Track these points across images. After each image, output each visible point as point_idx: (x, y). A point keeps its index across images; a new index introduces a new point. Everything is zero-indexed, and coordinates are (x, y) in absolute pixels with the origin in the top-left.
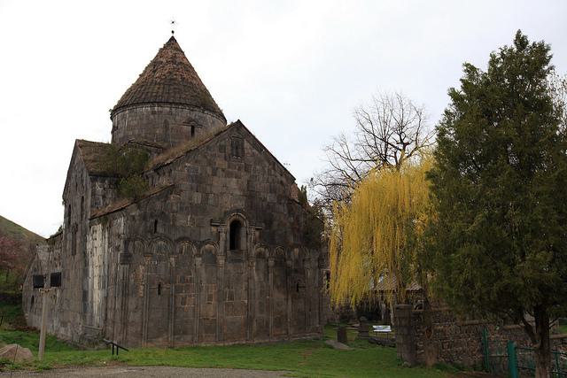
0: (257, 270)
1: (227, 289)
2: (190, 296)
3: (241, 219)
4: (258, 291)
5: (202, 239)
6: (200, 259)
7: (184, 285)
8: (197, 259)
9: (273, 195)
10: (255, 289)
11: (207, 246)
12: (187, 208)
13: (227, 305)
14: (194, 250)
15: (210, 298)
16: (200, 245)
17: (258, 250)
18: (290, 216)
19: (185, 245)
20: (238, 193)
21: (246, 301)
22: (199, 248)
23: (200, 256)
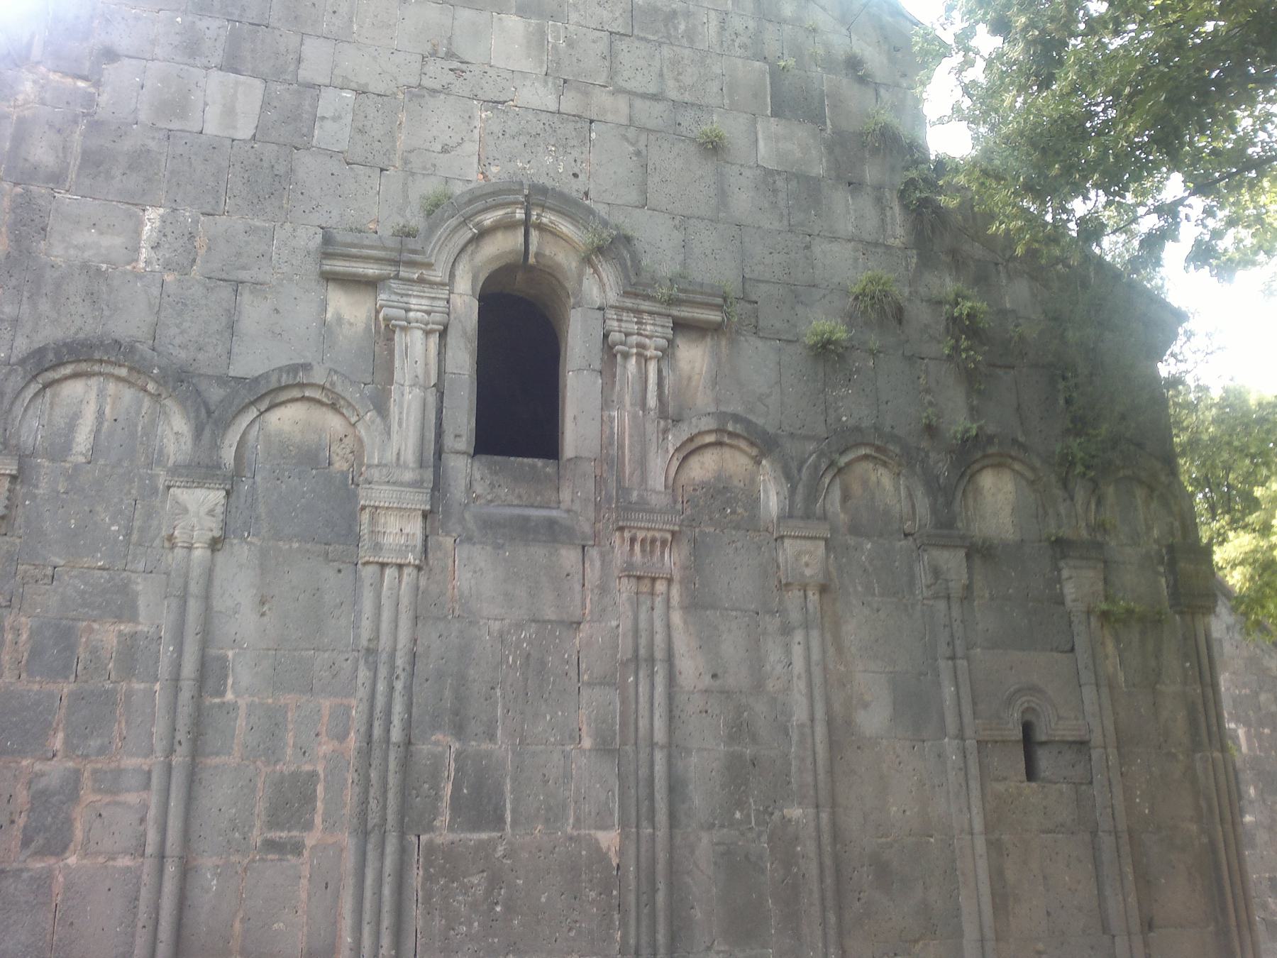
0: (694, 605)
1: (441, 745)
2: (111, 783)
3: (565, 259)
4: (704, 760)
5: (251, 362)
6: (215, 497)
7: (67, 688)
8: (185, 495)
9: (802, 132)
10: (674, 748)
11: (287, 419)
12: (139, 160)
13: (447, 865)
14: (175, 432)
15: (292, 802)
16: (219, 400)
17: (703, 467)
18: (927, 261)
19: (86, 403)
20: (538, 95)
21: (609, 839)
22: (210, 421)
23: (202, 470)
